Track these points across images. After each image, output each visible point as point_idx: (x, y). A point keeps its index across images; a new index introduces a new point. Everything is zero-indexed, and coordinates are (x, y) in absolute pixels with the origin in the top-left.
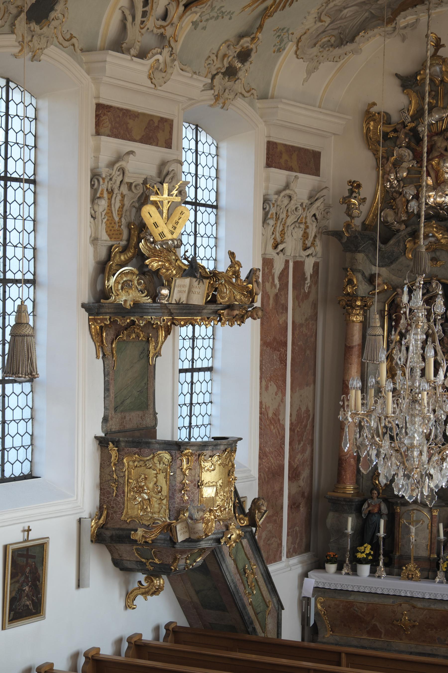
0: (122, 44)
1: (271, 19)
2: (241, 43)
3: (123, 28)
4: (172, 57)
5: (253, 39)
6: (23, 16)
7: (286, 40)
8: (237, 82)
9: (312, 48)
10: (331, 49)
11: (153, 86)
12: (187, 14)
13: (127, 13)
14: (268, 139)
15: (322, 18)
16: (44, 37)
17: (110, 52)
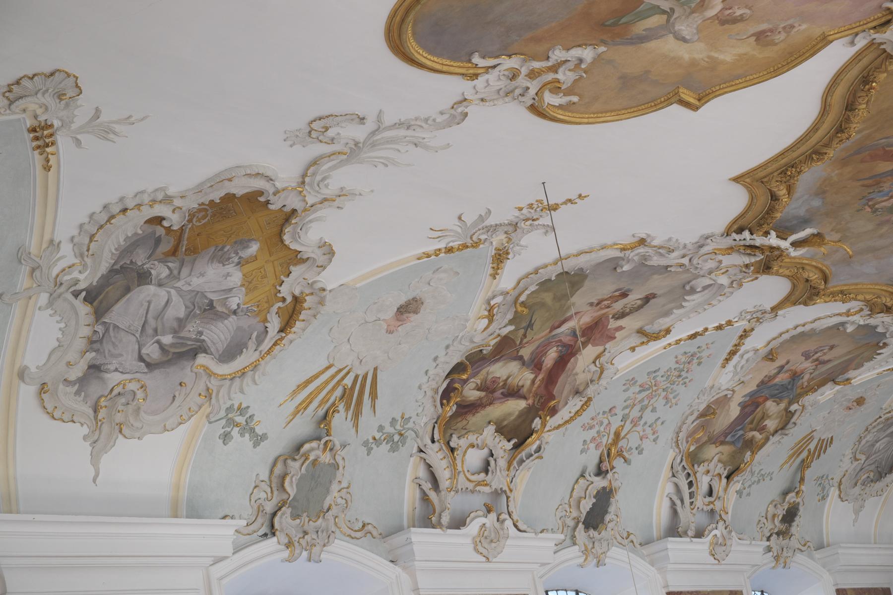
0: (678, 528)
1: (809, 469)
2: (787, 500)
3: (674, 512)
4: (728, 529)
5: (797, 493)
6: (581, 526)
7: (827, 487)
8: (791, 539)
9: (854, 487)
10: (872, 484)
11: (716, 562)
12: (730, 485)
13: (675, 498)
14: (836, 588)
15: (858, 457)
16: (604, 540)
17: (670, 539)
